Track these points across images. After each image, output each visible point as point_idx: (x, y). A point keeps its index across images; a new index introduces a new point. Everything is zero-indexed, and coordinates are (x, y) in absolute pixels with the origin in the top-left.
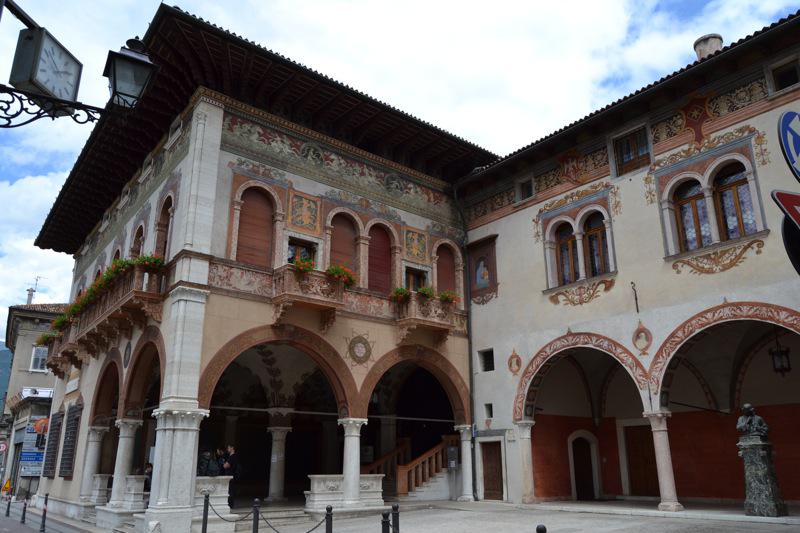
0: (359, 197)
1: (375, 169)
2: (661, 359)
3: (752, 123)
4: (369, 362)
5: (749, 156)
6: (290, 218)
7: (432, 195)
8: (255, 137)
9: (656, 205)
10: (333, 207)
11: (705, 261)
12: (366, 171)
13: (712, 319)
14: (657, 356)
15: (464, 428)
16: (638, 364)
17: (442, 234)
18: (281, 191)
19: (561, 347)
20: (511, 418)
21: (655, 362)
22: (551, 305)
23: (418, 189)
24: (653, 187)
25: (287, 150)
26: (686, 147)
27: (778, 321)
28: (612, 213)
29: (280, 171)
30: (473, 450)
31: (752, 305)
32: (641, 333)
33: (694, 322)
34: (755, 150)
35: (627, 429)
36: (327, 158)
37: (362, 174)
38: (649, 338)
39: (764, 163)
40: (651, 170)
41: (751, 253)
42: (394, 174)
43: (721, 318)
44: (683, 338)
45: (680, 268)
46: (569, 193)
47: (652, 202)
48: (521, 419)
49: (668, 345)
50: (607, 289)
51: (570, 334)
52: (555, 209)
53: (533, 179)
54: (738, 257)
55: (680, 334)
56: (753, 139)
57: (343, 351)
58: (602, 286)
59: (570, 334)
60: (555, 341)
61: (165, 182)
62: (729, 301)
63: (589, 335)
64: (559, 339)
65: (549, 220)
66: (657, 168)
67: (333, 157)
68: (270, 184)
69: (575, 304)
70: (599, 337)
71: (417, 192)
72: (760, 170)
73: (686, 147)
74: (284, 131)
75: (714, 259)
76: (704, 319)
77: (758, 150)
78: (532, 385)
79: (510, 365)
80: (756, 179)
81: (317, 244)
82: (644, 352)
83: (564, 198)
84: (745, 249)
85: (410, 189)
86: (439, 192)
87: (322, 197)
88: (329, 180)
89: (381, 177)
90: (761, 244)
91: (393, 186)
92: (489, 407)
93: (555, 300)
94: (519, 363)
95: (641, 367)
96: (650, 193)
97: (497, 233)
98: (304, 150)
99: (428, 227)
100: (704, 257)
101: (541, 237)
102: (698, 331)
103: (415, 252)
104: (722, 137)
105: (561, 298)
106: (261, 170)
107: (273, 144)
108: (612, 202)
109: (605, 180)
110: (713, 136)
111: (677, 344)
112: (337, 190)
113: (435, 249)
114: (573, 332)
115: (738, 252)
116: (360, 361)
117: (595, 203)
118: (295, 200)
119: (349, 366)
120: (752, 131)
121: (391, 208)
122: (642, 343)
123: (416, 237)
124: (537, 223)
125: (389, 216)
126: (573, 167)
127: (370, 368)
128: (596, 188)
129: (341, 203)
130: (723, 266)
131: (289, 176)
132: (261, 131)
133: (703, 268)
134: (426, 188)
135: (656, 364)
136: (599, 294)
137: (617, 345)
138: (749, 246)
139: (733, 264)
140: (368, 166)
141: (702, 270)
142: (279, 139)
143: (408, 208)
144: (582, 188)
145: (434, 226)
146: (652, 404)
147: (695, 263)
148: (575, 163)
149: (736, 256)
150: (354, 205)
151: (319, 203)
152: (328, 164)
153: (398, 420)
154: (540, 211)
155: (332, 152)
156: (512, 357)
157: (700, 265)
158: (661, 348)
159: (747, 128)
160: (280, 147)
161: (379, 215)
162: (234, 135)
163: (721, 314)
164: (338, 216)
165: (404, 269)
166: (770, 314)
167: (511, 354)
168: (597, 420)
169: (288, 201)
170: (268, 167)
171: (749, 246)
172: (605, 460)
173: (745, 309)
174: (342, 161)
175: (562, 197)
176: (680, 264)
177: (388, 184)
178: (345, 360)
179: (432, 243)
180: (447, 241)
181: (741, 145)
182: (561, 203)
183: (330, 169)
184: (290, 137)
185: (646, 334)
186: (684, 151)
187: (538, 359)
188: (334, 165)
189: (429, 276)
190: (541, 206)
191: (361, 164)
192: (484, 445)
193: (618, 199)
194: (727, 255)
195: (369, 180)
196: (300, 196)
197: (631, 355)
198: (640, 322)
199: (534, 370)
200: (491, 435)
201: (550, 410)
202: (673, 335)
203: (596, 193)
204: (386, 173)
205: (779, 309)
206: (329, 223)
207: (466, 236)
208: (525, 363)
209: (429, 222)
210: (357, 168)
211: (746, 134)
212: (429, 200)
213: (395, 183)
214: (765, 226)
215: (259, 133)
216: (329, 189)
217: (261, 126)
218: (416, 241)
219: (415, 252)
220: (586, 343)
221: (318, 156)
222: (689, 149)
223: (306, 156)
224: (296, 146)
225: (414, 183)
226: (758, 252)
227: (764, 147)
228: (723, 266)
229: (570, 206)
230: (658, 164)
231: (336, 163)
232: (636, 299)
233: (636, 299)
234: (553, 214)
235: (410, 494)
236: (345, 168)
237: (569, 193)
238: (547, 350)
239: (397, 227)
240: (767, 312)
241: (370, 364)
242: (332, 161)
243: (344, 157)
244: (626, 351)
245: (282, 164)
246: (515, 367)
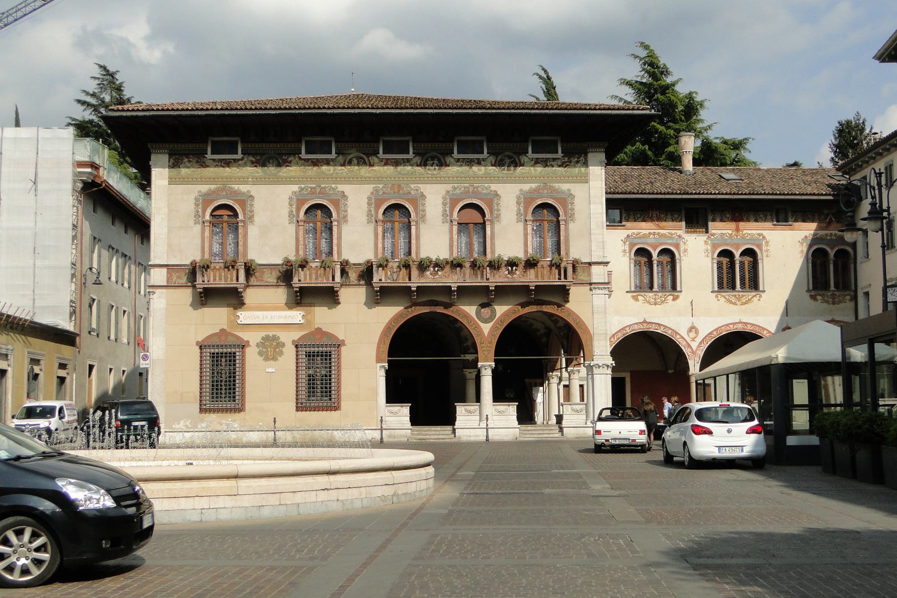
3: (765, 233)
5: (761, 249)
9: (710, 259)
13: (732, 329)
14: (700, 343)
16: (689, 346)
21: (699, 346)
22: (633, 301)
24: (709, 248)
26: (730, 232)
30: (558, 390)
31: (753, 325)
32: (692, 328)
34: (764, 248)
38: (697, 332)
41: (755, 299)
44: (716, 336)
50: (674, 300)
51: (645, 322)
52: (640, 238)
54: (749, 300)
55: (715, 333)
58: (671, 297)
63: (659, 325)
70: (665, 327)
72: (765, 259)
73: (730, 232)
82: (693, 339)
90: (761, 297)
95: (691, 348)
108: (682, 248)
109: (679, 232)
110: (745, 232)
117: (671, 244)
120: (764, 237)
122: (692, 334)
137: (677, 333)
139: (746, 303)
141: (731, 302)
154: (628, 236)
173: (749, 326)
175: (647, 232)
181: (757, 242)
182: (645, 236)
190: (630, 232)
202: (711, 333)
203: (672, 238)
205: (764, 329)
229: (652, 239)
230: (713, 235)
234: (638, 241)
238: (627, 329)
244: (682, 337)
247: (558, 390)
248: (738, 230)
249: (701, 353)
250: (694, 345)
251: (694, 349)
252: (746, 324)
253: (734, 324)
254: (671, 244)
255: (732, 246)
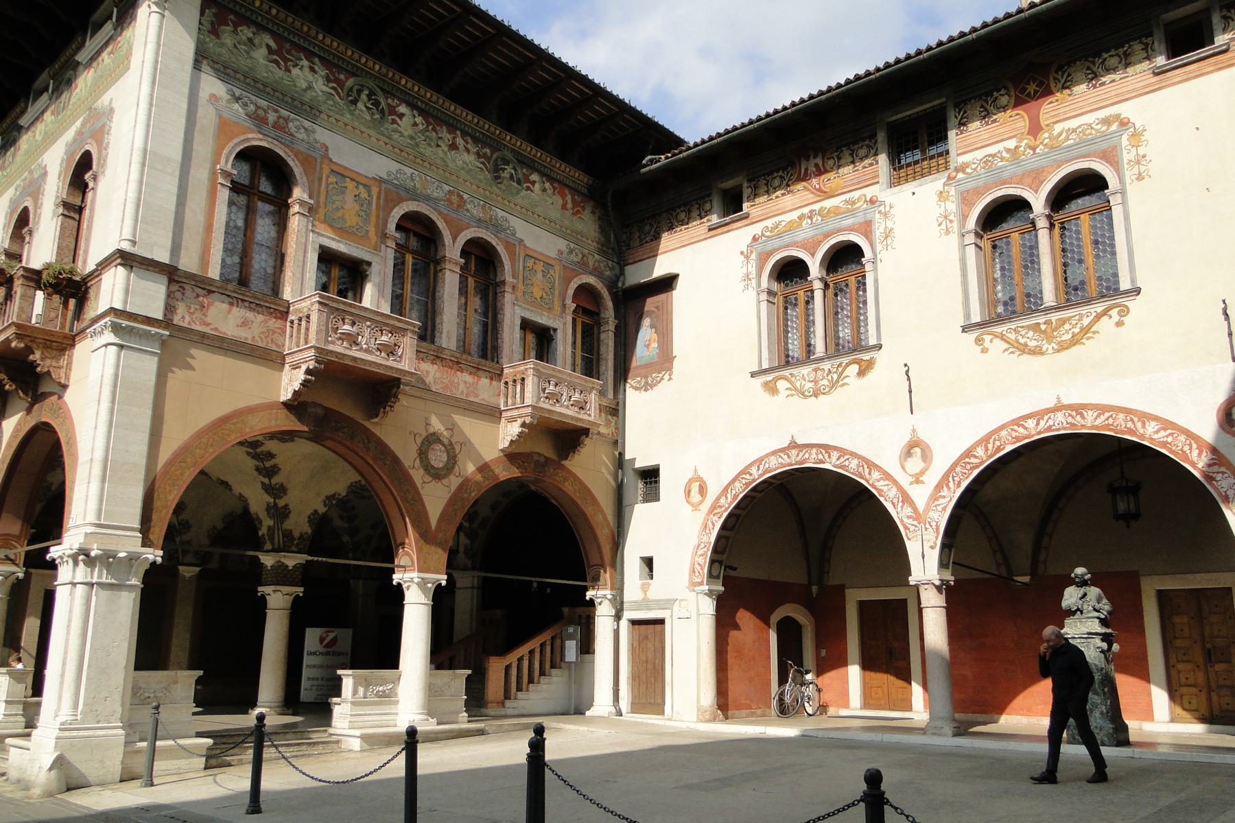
0: (447, 188)
1: (476, 140)
2: (945, 492)
3: (1124, 110)
4: (452, 477)
6: (322, 211)
7: (569, 198)
8: (260, 54)
9: (954, 238)
10: (400, 200)
11: (1031, 334)
12: (460, 141)
13: (1034, 431)
14: (939, 487)
15: (600, 594)
16: (906, 499)
17: (583, 266)
18: (307, 161)
19: (777, 465)
20: (686, 583)
21: (935, 496)
22: (766, 396)
23: (547, 185)
24: (952, 206)
25: (320, 86)
26: (1011, 144)
27: (1142, 436)
28: (879, 247)
29: (307, 124)
30: (617, 633)
31: (1102, 409)
32: (914, 446)
33: (1004, 433)
34: (1127, 156)
35: (863, 606)
36: (392, 111)
37: (453, 147)
38: (927, 456)
39: (1140, 177)
40: (949, 178)
41: (1106, 324)
42: (509, 155)
43: (1049, 429)
44: (984, 458)
45: (987, 344)
46: (806, 210)
47: (948, 232)
48: (701, 584)
49: (958, 469)
50: (861, 373)
51: (793, 445)
52: (779, 235)
53: (745, 185)
54: (1086, 330)
55: (980, 452)
56: (1125, 138)
57: (408, 455)
59: (793, 445)
60: (767, 456)
61: (78, 124)
62: (1065, 401)
63: (827, 448)
64: (774, 453)
65: (769, 254)
66: (960, 175)
67: (403, 109)
68: (287, 146)
69: (806, 397)
70: (842, 452)
71: (544, 190)
72: (1132, 189)
73: (1011, 144)
74: (316, 50)
75: (1044, 332)
76: (1021, 430)
77: (1132, 156)
78: (723, 527)
79: (688, 493)
80: (1124, 203)
81: (369, 264)
82: (917, 480)
83: (793, 215)
84: (1098, 317)
85: (533, 183)
86: (580, 193)
87: (380, 181)
88: (398, 153)
89: (485, 156)
90: (1125, 311)
91: (506, 175)
92: (649, 562)
93: (771, 388)
94: (703, 490)
96: (946, 217)
97: (674, 271)
98: (351, 89)
99: (561, 252)
100: (1029, 328)
101: (754, 282)
102: (1009, 448)
103: (537, 293)
104: (1074, 131)
105: (782, 385)
106: (272, 117)
107: (296, 71)
108: (878, 231)
109: (869, 192)
110: (1058, 128)
111: (973, 469)
112: (409, 171)
113: (571, 292)
114: (799, 442)
115: (1086, 321)
116: (437, 475)
117: (851, 229)
118: (333, 179)
119: (418, 482)
120: (1124, 124)
121: (500, 213)
122: (915, 464)
123: (540, 266)
124: (747, 257)
125: (497, 227)
126: (817, 165)
127: (453, 489)
128: (854, 203)
129: (414, 195)
130: (1059, 343)
131: (323, 135)
132: (273, 44)
133: (1026, 345)
134: (559, 184)
135: (936, 499)
136: (846, 381)
137: (872, 465)
138: (1105, 313)
139: (1075, 341)
140: (464, 134)
141: (1024, 349)
142: (305, 63)
143: (529, 215)
144: (828, 203)
145: (571, 252)
146: (925, 563)
147: (1012, 336)
148: (819, 161)
149: (1082, 329)
150: (437, 200)
151: (375, 191)
152: (394, 122)
153: (485, 578)
154: (755, 239)
155: (402, 101)
156: (691, 481)
157: (1022, 341)
158: (946, 477)
159: (1117, 117)
160: (307, 78)
161: (480, 222)
162: (222, 45)
163: (1051, 422)
164: (406, 217)
165: (518, 322)
166: (1130, 425)
167: (690, 475)
168: (814, 589)
169: (320, 179)
170: (284, 113)
171: (1105, 313)
172: (823, 653)
173: (1090, 415)
174: (419, 120)
175: (794, 215)
176: (987, 338)
177: (496, 171)
178: (411, 472)
179: (567, 281)
180: (591, 280)
181: (1103, 146)
182: (792, 227)
183: (396, 131)
184: (326, 62)
185: (923, 451)
186: (1008, 151)
187: (737, 484)
188: (405, 123)
189: (559, 336)
190: (757, 229)
191: (452, 128)
192: (634, 622)
193: (890, 224)
194: (1067, 326)
195: (466, 159)
196: (341, 174)
197: (895, 482)
198: (914, 431)
199: (728, 504)
200: (650, 609)
201: (746, 571)
202: (968, 453)
204: (494, 150)
205: (1145, 417)
206: (392, 227)
207: (622, 273)
208: (713, 492)
209: (562, 244)
210: (445, 133)
211: (1114, 127)
212: (564, 207)
213: (509, 170)
214: (1133, 281)
215: (268, 46)
216: (394, 166)
217: (274, 35)
218: (540, 275)
219: (537, 293)
220: (822, 462)
221: (377, 104)
222: (1017, 147)
223: (354, 102)
224: (337, 81)
225: (542, 174)
226: (1119, 324)
227: (1141, 151)
228: (1059, 343)
229: (806, 232)
230: (962, 168)
231: (408, 121)
232: (910, 392)
233: (910, 392)
234: (776, 243)
235: (508, 703)
236: (423, 132)
237: (806, 210)
238: (754, 470)
239: (508, 246)
240: (1126, 421)
241: (454, 482)
242: (401, 116)
243: (422, 112)
244: (887, 476)
245: (310, 110)
246: (695, 496)
247: (617, 633)
248: (1035, 129)
249: (941, 518)
250: (920, 495)
251: (921, 505)
252: (1079, 409)
253: (1038, 415)
254: (851, 229)
255: (1019, 181)
